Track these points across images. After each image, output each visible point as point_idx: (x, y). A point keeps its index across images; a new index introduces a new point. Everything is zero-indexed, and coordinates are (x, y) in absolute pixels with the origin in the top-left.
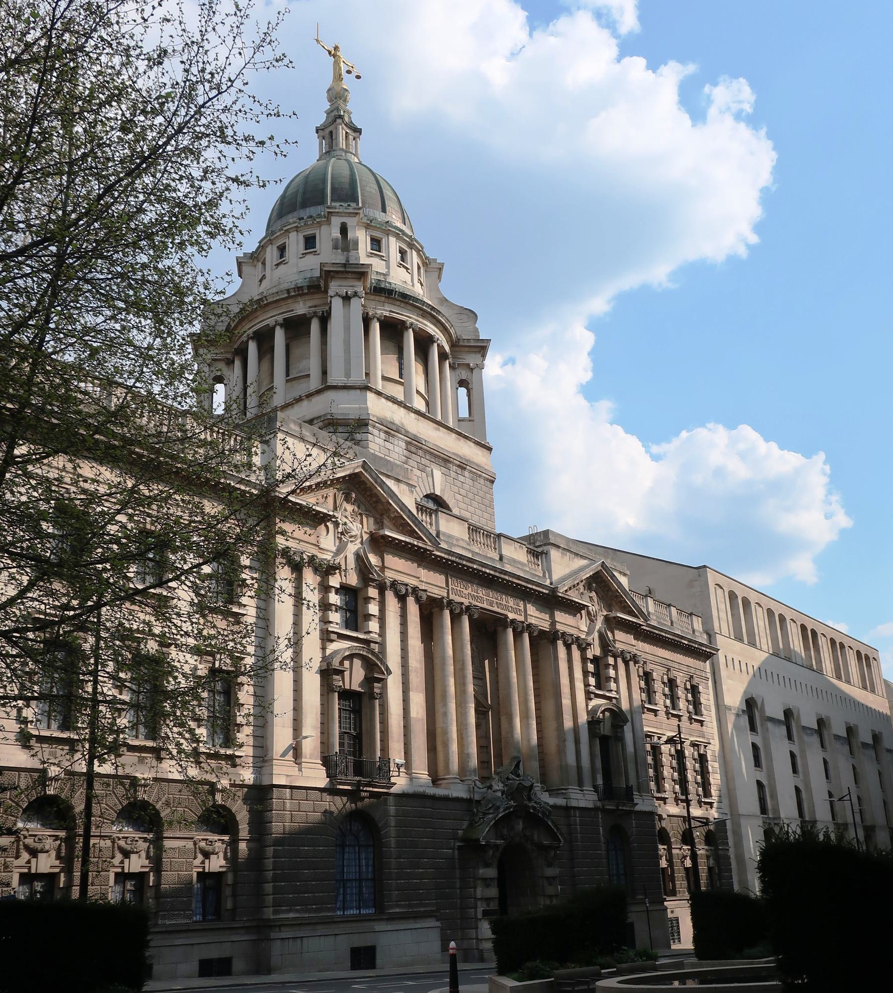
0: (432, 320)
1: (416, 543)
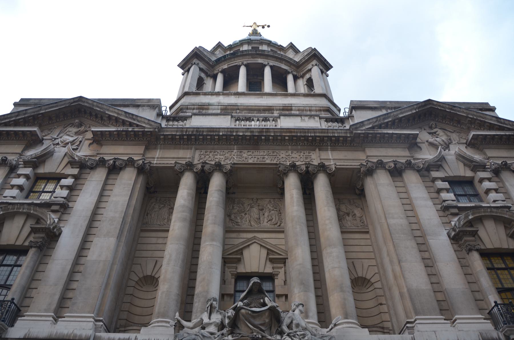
0: (262, 57)
1: (130, 130)
